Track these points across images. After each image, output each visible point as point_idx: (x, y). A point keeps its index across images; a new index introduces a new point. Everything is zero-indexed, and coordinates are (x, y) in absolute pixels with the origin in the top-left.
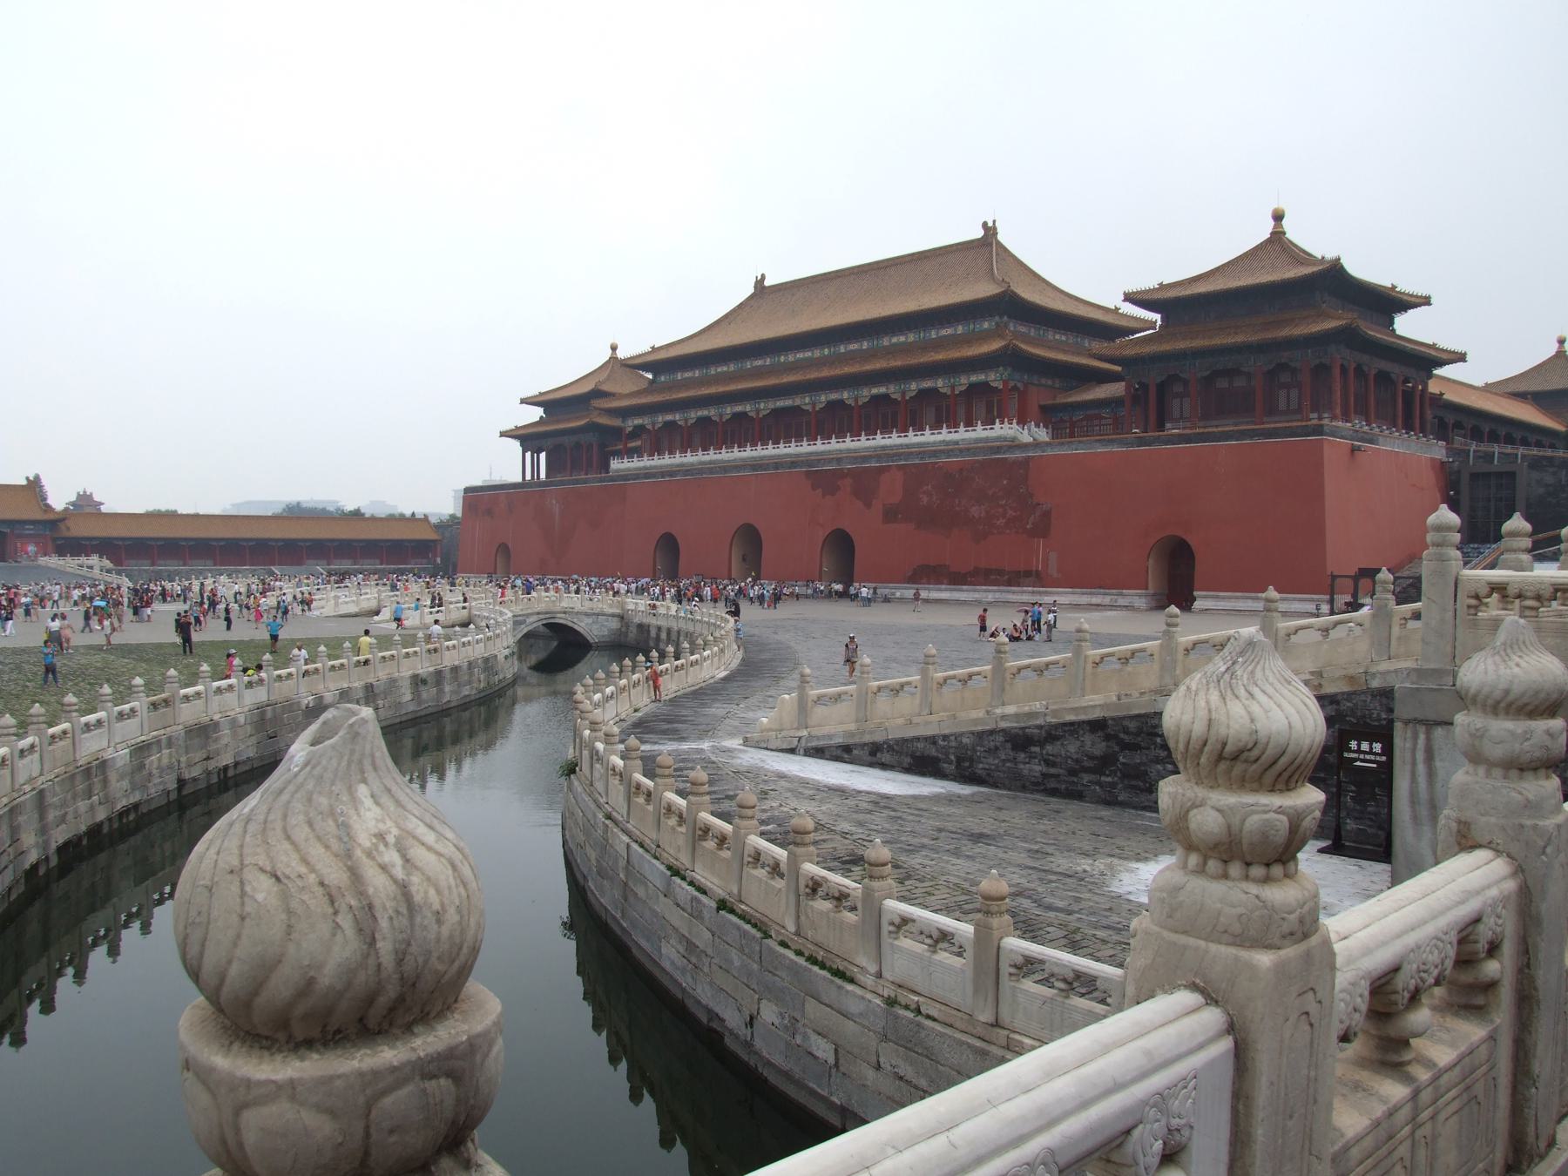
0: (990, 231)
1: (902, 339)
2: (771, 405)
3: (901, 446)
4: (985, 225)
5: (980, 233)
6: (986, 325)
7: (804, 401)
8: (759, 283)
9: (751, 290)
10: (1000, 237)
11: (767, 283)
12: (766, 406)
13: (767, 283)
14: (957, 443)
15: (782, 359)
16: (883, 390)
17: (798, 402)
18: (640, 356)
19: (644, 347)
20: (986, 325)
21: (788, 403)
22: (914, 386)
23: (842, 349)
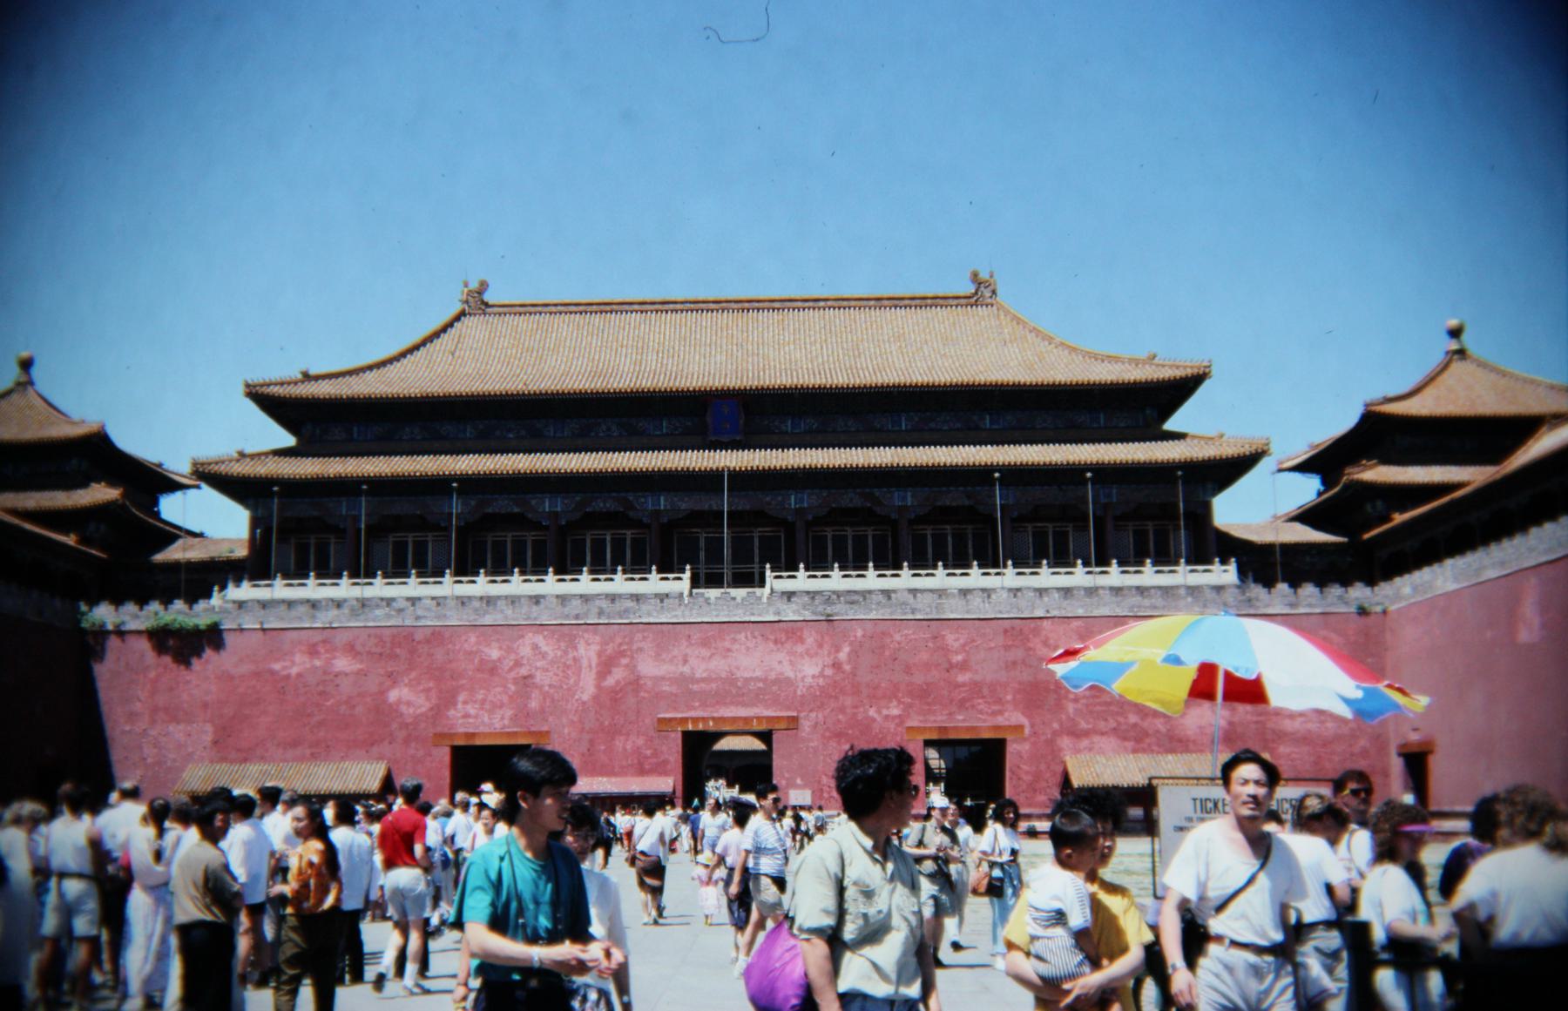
4: (975, 277)
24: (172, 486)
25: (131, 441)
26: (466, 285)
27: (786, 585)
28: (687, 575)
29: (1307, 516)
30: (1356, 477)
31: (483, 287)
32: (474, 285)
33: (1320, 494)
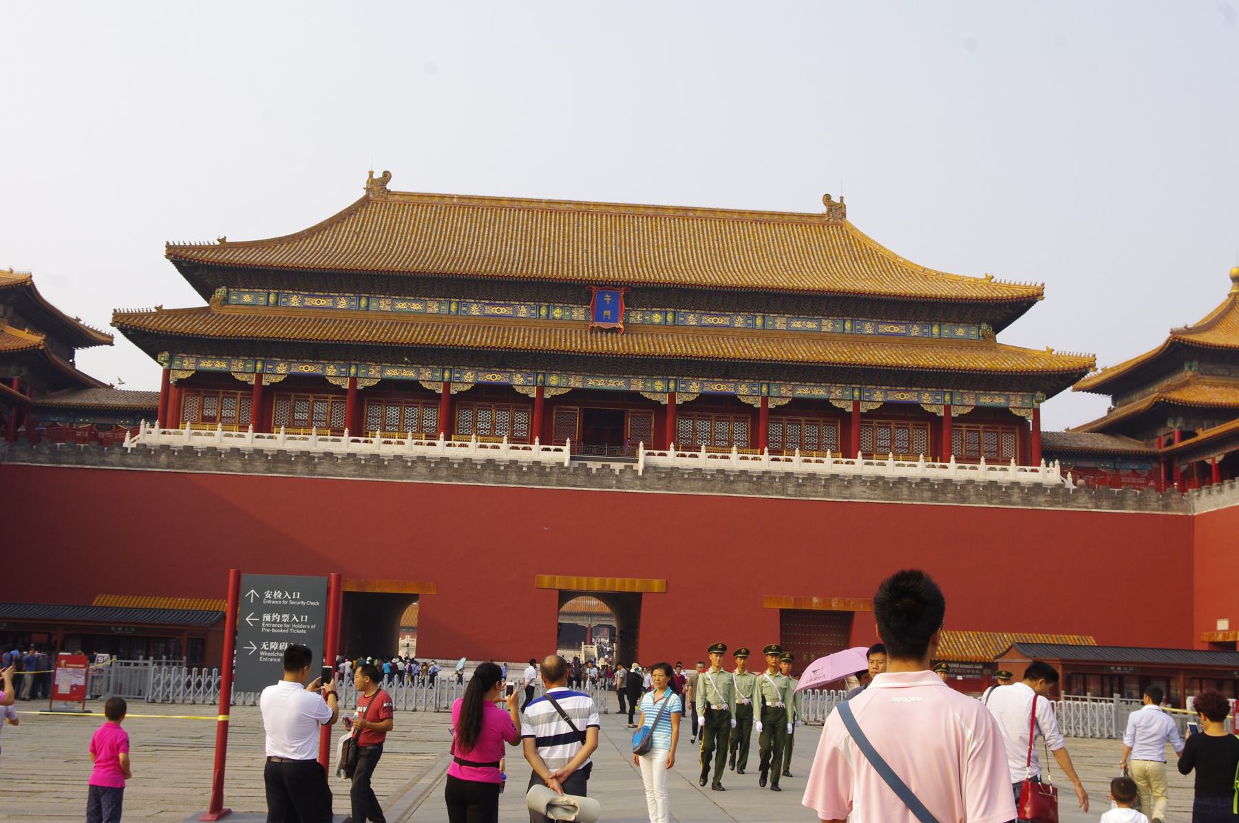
0: (836, 210)
1: (811, 325)
2: (576, 382)
5: (822, 209)
8: (378, 186)
10: (852, 217)
11: (389, 186)
12: (558, 384)
13: (389, 186)
15: (557, 313)
16: (819, 392)
17: (637, 385)
18: (200, 248)
19: (208, 237)
20: (960, 332)
24: (89, 338)
25: (50, 293)
26: (371, 173)
27: (658, 460)
28: (566, 449)
29: (1108, 428)
30: (1175, 396)
31: (387, 176)
32: (378, 175)
33: (1110, 411)
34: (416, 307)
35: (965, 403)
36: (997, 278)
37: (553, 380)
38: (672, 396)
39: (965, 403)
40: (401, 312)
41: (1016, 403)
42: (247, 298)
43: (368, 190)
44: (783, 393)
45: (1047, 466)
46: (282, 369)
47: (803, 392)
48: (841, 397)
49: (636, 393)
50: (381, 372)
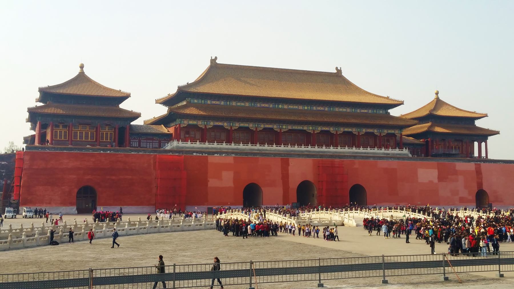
0: (339, 71)
2: (290, 127)
3: (365, 153)
4: (337, 68)
5: (335, 71)
6: (381, 112)
7: (309, 129)
8: (213, 61)
9: (208, 64)
10: (343, 74)
12: (285, 128)
14: (389, 154)
15: (280, 106)
16: (350, 130)
17: (305, 128)
20: (381, 112)
21: (300, 128)
22: (364, 130)
23: (315, 108)
31: (216, 58)
32: (213, 58)
34: (243, 104)
35: (386, 131)
36: (391, 97)
37: (284, 127)
38: (314, 131)
39: (386, 131)
40: (239, 106)
41: (397, 132)
42: (196, 101)
43: (211, 62)
44: (342, 130)
45: (406, 149)
46: (212, 123)
47: (346, 130)
48: (354, 130)
49: (305, 130)
50: (239, 124)
